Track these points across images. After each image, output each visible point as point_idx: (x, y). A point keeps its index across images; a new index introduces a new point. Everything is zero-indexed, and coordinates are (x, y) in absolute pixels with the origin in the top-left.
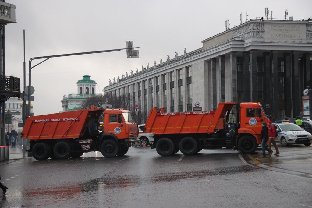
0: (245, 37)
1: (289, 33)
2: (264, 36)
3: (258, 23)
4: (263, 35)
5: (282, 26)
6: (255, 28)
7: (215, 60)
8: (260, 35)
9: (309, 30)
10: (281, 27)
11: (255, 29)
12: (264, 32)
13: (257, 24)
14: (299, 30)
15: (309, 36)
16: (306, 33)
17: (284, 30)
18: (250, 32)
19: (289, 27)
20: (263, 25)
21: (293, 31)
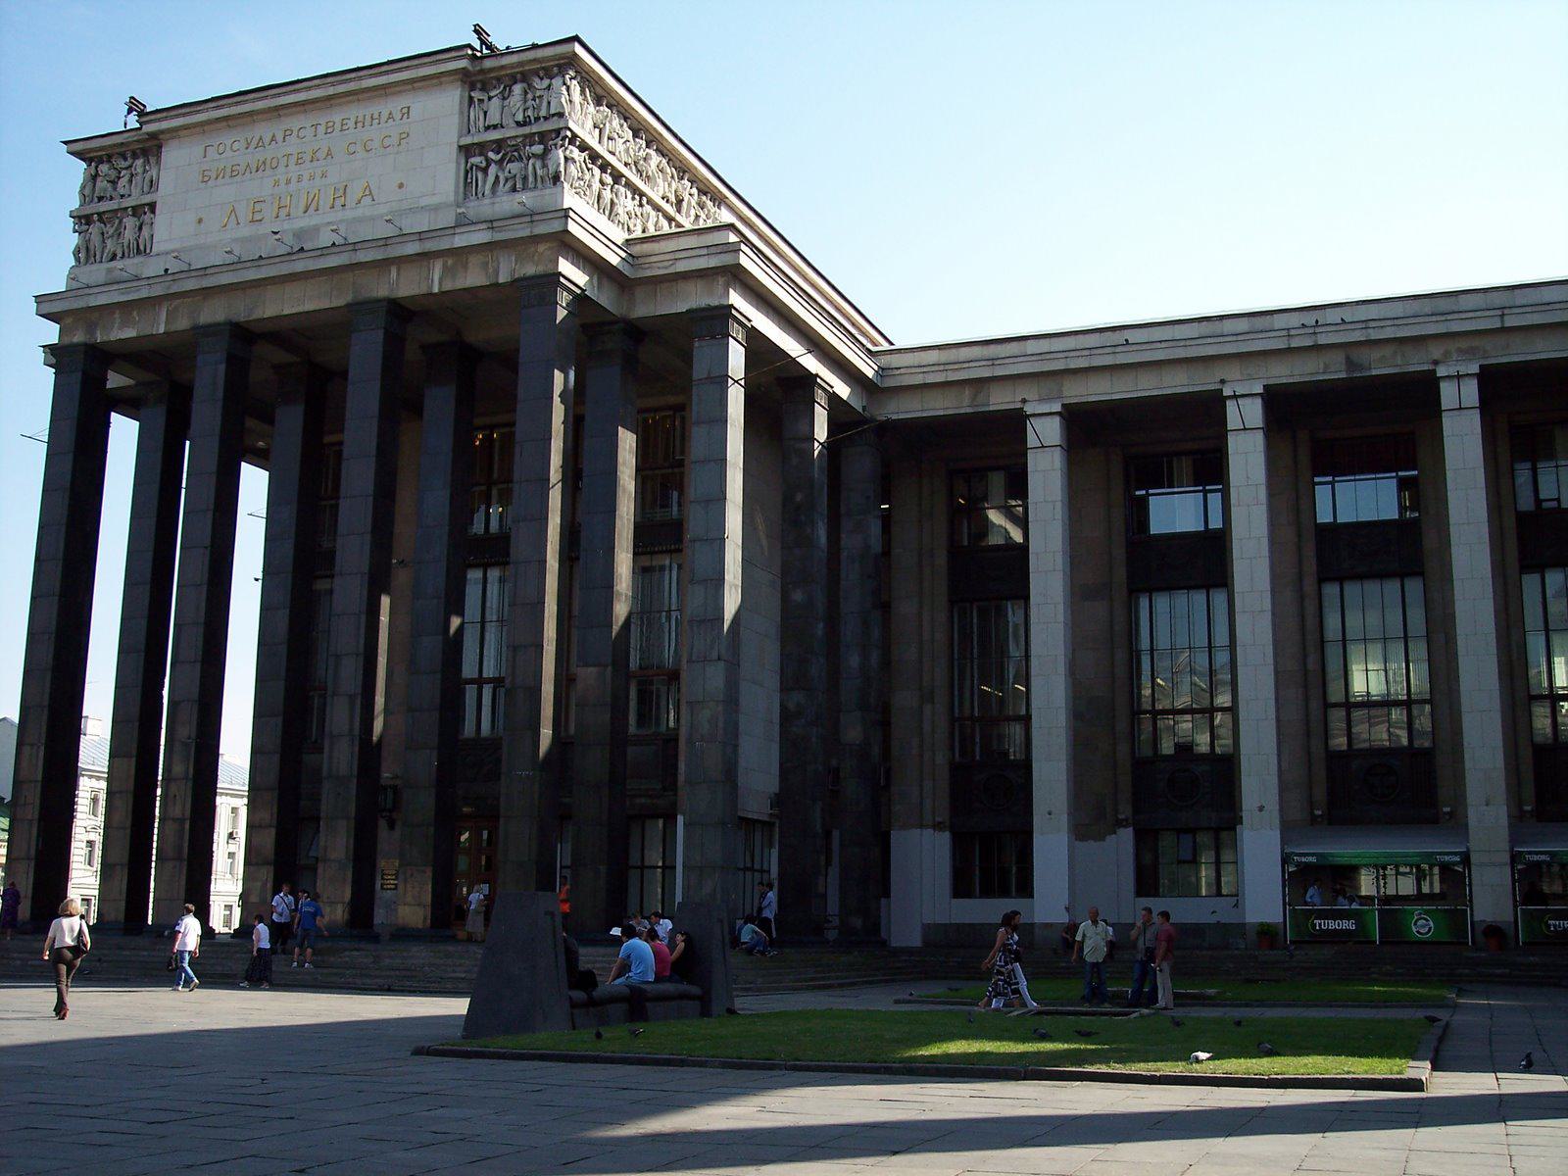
1: (324, 175)
5: (280, 136)
8: (129, 234)
9: (494, 118)
15: (493, 169)
21: (361, 153)
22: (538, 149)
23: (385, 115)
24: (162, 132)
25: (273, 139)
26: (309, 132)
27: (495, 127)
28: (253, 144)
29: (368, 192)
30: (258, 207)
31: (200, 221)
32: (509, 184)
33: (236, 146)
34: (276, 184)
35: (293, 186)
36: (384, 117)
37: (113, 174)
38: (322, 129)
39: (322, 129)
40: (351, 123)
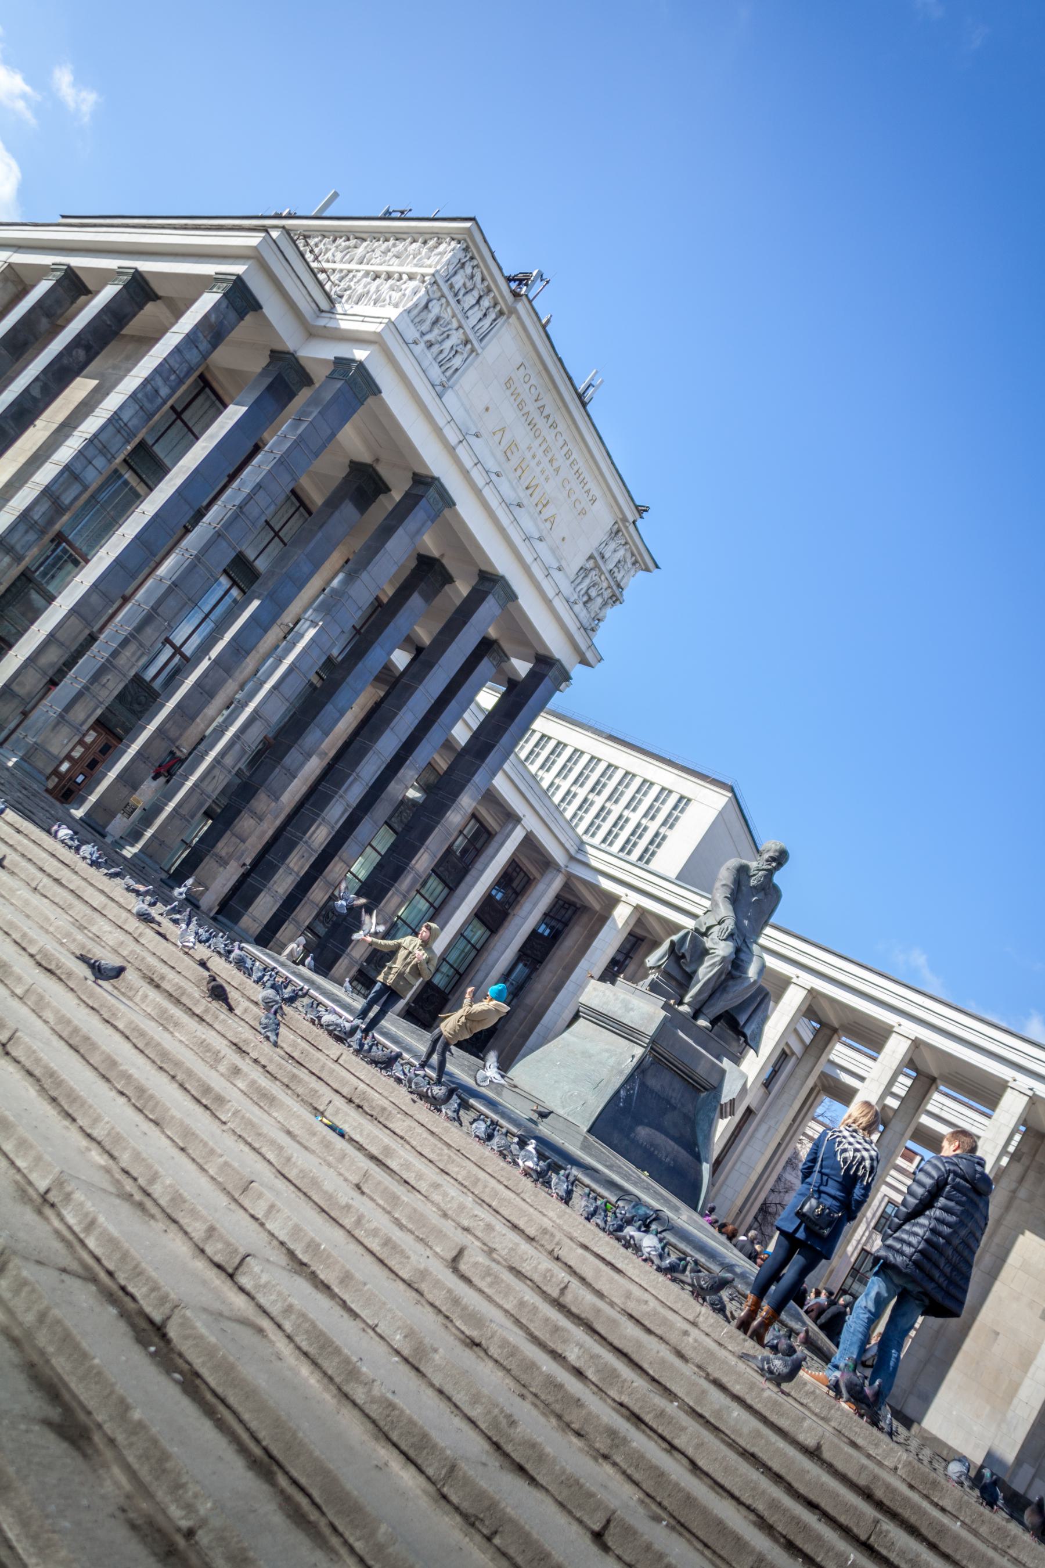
0: (360, 289)
1: (547, 479)
2: (457, 370)
3: (483, 280)
4: (457, 362)
6: (459, 280)
7: (73, 287)
8: (447, 345)
10: (548, 417)
11: (451, 287)
12: (473, 350)
13: (478, 278)
14: (583, 512)
16: (591, 557)
17: (544, 447)
18: (411, 277)
19: (568, 455)
20: (492, 315)
22: (607, 594)
23: (586, 488)
24: (519, 318)
25: (548, 417)
26: (561, 443)
27: (603, 557)
28: (540, 403)
29: (551, 520)
30: (513, 447)
31: (487, 409)
32: (585, 598)
33: (533, 389)
34: (529, 448)
35: (533, 463)
36: (586, 488)
37: (469, 285)
38: (565, 449)
39: (565, 449)
40: (576, 468)
